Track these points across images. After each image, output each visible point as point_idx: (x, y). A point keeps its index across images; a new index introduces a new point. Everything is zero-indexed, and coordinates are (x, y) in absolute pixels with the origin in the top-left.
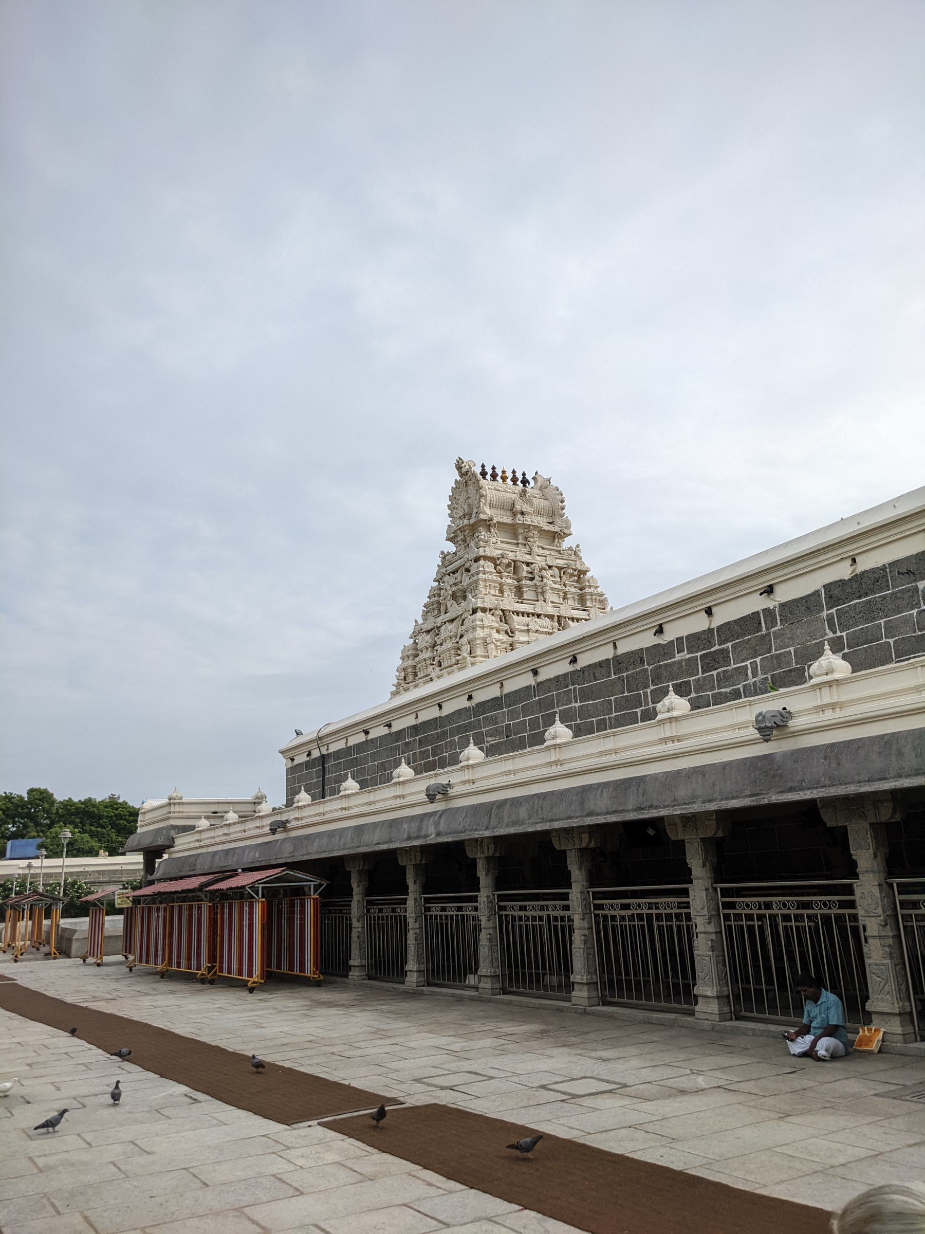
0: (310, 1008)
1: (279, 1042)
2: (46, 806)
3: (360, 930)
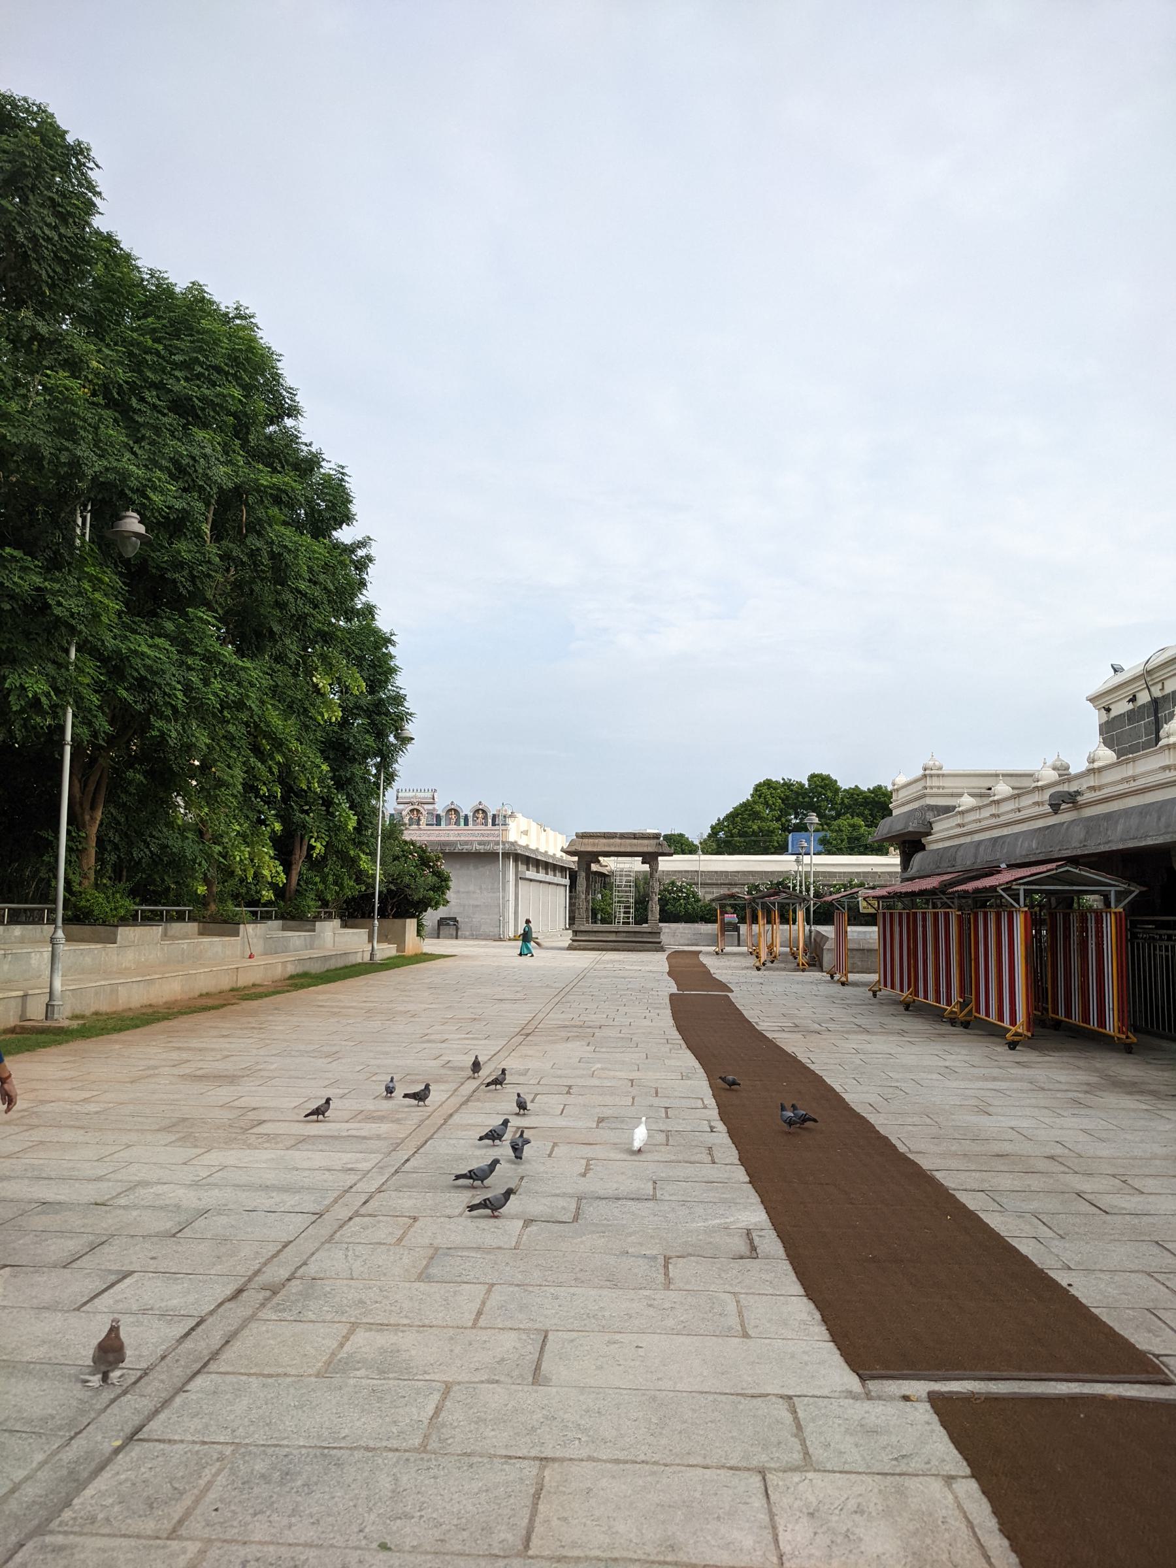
0: (1090, 1089)
1: (996, 1148)
2: (829, 794)
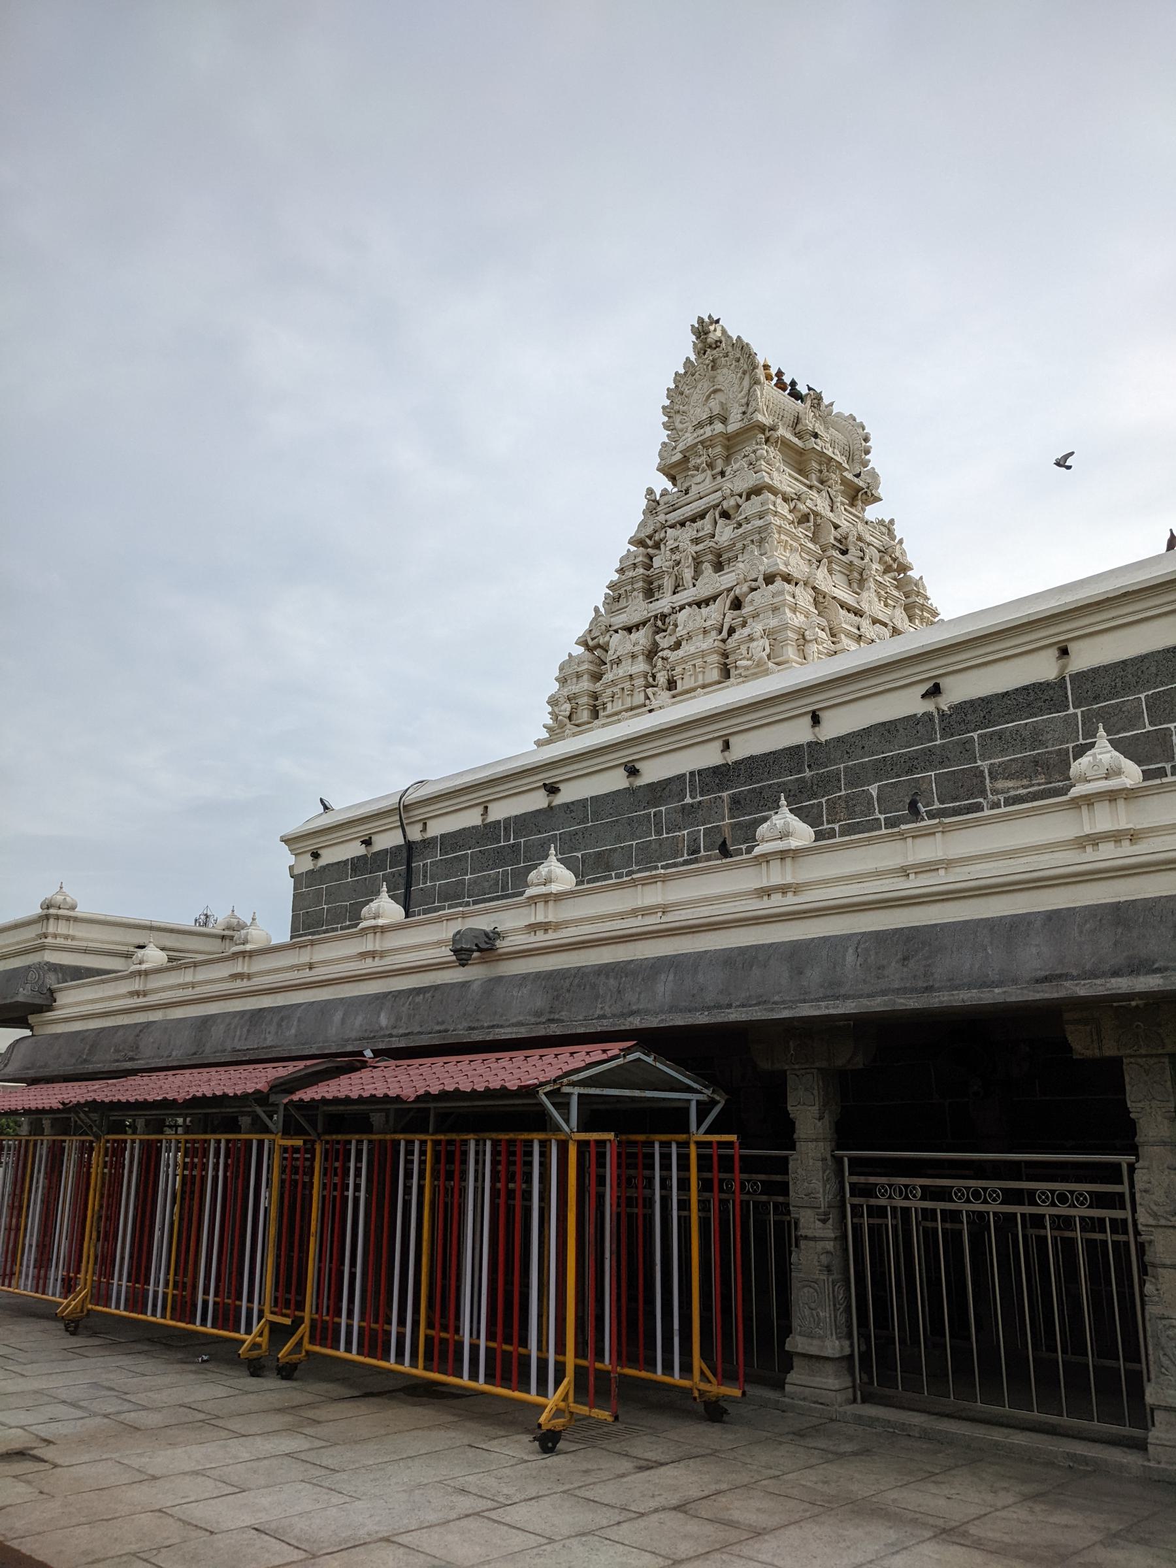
3: (830, 1246)
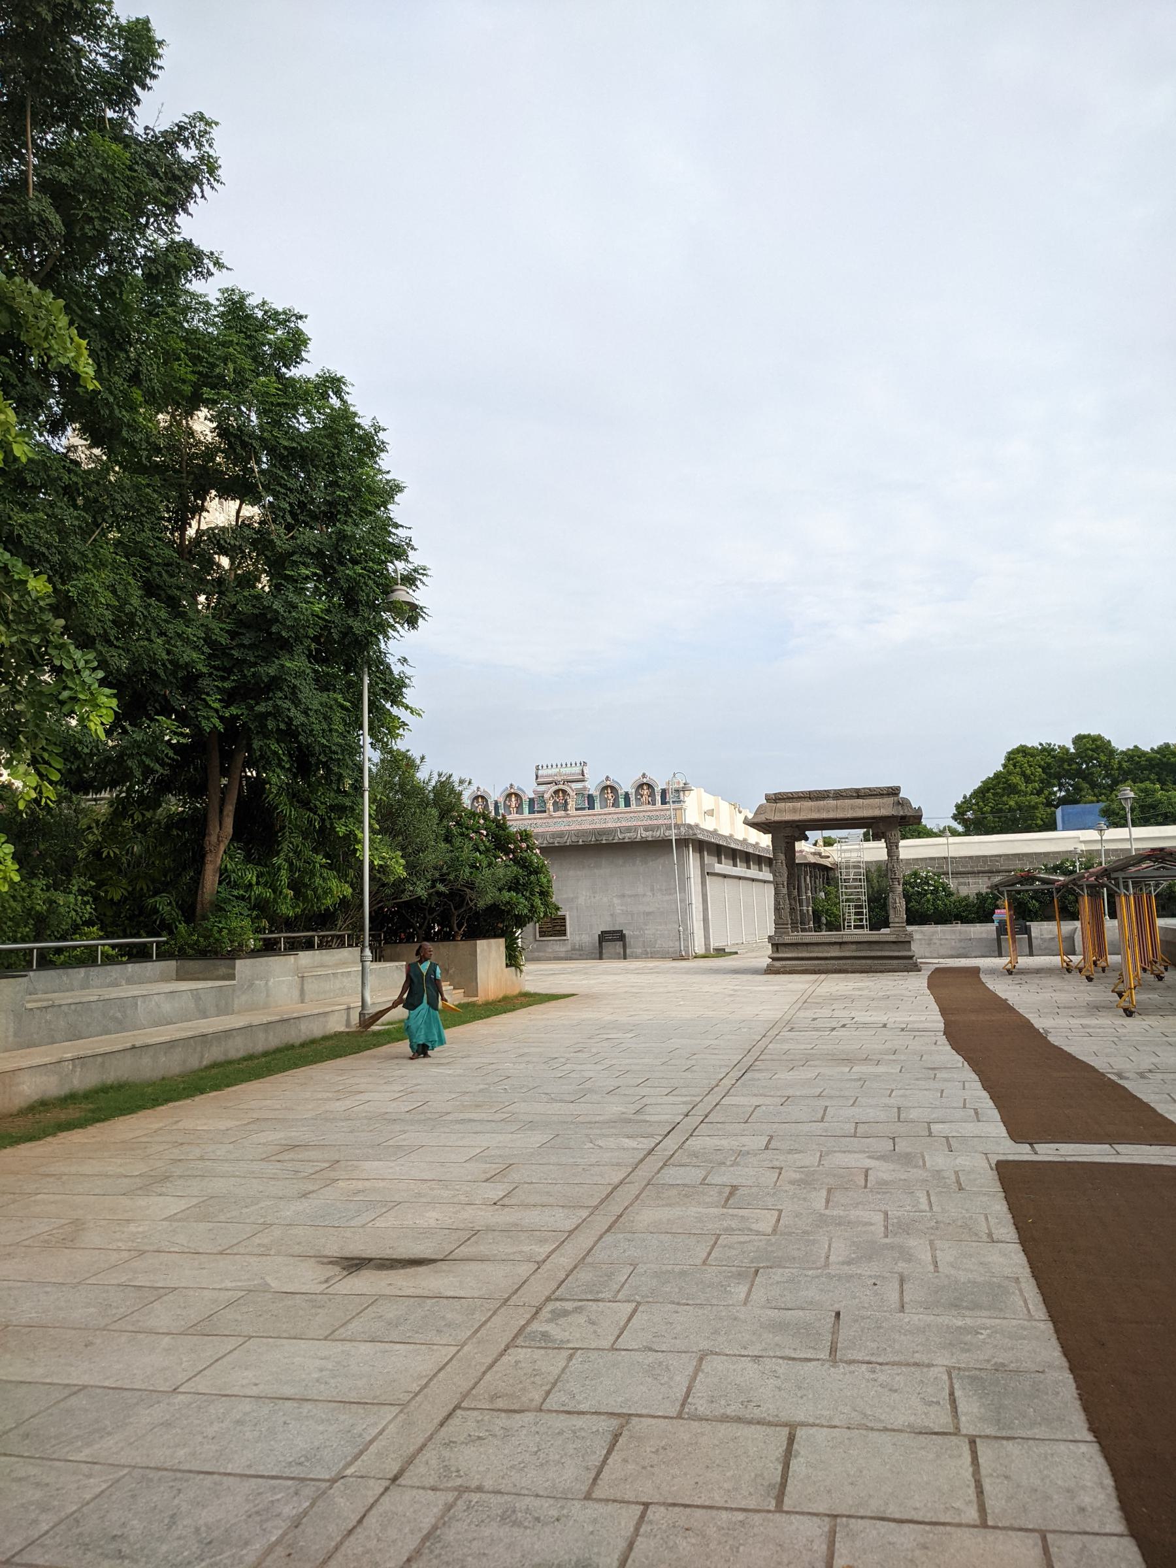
2: (1103, 758)
